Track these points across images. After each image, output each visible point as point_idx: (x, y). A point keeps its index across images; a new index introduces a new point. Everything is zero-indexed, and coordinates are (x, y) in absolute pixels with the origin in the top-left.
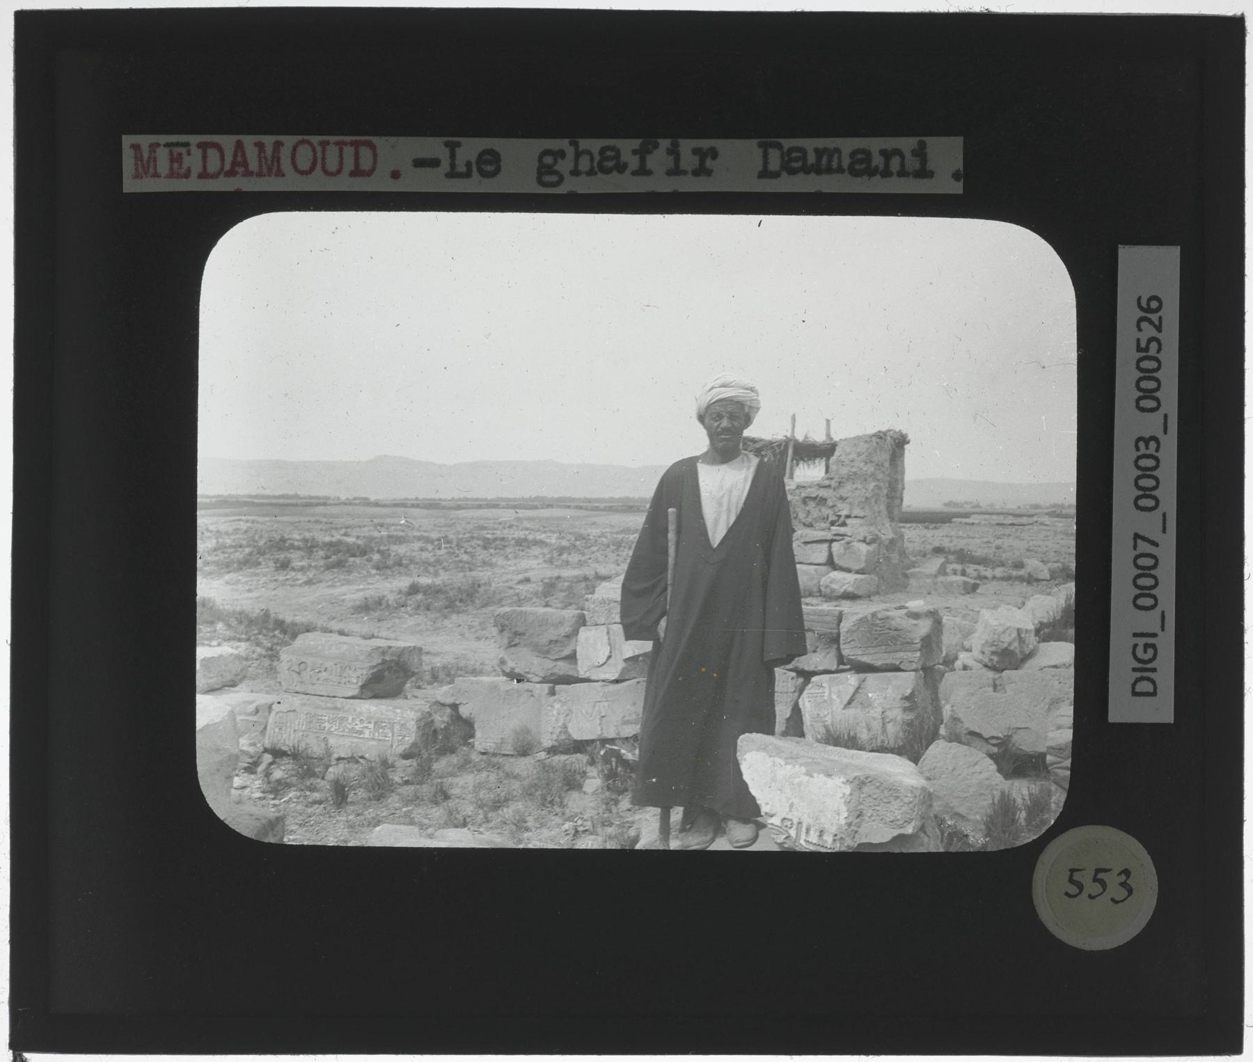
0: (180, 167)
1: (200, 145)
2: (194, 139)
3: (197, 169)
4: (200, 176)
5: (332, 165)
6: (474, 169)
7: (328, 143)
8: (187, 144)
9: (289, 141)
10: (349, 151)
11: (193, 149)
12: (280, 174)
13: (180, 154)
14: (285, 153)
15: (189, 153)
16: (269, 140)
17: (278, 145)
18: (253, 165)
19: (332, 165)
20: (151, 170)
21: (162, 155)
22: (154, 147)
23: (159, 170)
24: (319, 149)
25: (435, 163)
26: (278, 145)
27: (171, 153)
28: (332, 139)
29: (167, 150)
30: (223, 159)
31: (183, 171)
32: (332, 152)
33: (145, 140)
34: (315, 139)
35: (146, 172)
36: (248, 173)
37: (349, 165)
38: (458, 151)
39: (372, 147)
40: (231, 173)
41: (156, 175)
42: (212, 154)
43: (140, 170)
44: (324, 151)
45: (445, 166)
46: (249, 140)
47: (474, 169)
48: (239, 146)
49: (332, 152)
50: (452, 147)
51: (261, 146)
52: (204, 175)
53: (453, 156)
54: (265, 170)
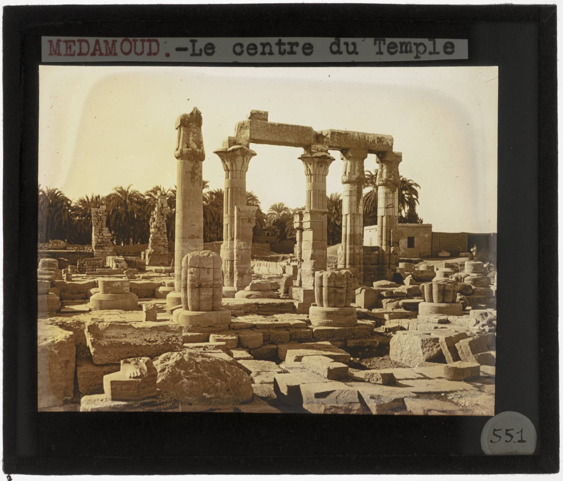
0: (71, 51)
1: (79, 41)
2: (76, 38)
3: (77, 51)
4: (79, 55)
5: (139, 50)
6: (203, 53)
7: (137, 40)
8: (74, 41)
9: (120, 40)
10: (147, 44)
11: (76, 41)
12: (116, 54)
13: (70, 45)
14: (118, 45)
15: (75, 45)
16: (110, 39)
17: (114, 42)
18: (103, 51)
19: (139, 50)
20: (57, 52)
21: (63, 46)
22: (59, 41)
23: (61, 52)
24: (133, 43)
25: (185, 49)
26: (114, 42)
27: (67, 45)
28: (139, 39)
29: (65, 44)
30: (89, 47)
31: (72, 53)
32: (139, 44)
33: (54, 39)
34: (131, 39)
35: (55, 53)
36: (101, 54)
37: (147, 50)
38: (196, 44)
39: (157, 41)
40: (93, 54)
41: (59, 54)
42: (84, 44)
43: (53, 52)
44: (135, 44)
45: (190, 51)
46: (101, 39)
47: (203, 53)
48: (97, 42)
49: (139, 44)
50: (194, 42)
51: (106, 41)
52: (80, 54)
53: (194, 45)
54: (108, 52)
